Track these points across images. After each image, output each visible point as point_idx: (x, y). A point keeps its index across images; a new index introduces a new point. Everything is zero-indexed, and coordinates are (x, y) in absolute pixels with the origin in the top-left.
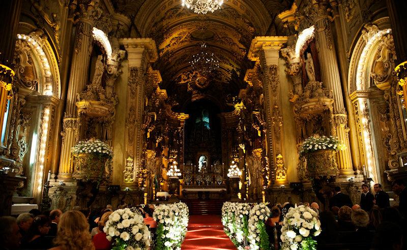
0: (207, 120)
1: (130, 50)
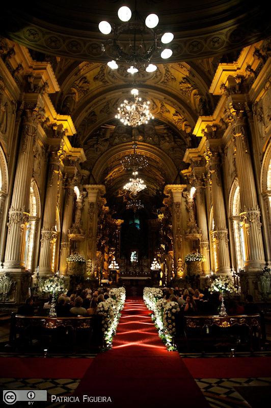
0: (137, 222)
1: (89, 191)
